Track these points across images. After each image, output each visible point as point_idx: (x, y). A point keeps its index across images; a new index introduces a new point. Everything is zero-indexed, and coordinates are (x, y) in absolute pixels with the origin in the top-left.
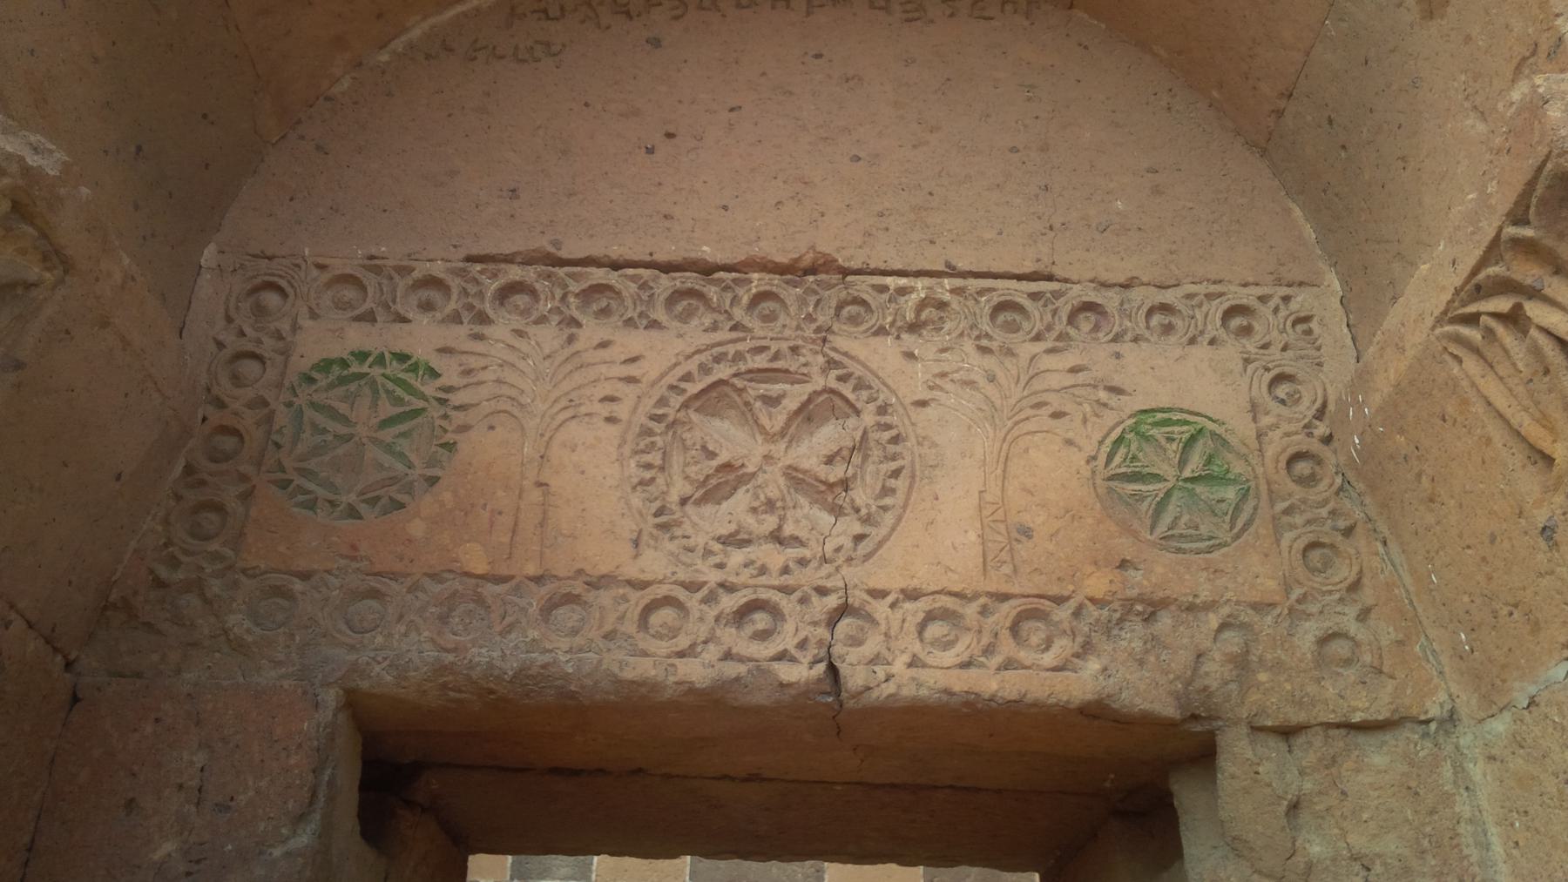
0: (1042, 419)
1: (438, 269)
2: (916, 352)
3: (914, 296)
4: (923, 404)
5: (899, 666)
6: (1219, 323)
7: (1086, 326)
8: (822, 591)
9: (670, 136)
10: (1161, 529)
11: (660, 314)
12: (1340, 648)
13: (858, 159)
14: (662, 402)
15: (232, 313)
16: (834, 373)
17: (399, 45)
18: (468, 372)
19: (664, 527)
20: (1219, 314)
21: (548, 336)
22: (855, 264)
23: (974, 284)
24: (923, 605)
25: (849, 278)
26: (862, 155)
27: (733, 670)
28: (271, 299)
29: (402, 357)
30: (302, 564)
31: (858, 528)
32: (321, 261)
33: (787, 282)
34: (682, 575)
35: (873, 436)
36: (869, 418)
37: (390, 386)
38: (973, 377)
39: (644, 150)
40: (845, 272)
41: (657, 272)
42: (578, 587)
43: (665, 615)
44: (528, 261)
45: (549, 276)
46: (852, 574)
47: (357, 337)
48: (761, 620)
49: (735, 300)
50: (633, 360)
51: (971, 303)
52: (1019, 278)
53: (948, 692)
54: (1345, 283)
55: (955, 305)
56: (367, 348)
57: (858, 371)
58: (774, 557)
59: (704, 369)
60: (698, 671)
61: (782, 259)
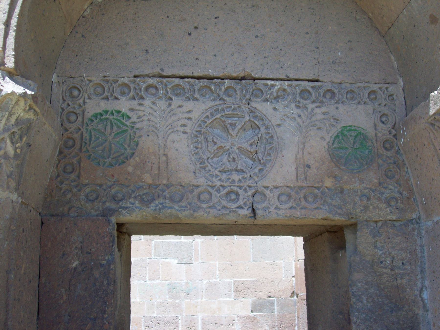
1: (126, 80)
2: (277, 107)
3: (276, 88)
6: (367, 96)
7: (328, 96)
8: (250, 187)
9: (196, 28)
11: (197, 95)
13: (257, 36)
15: (65, 98)
18: (139, 117)
20: (367, 94)
21: (162, 104)
22: (257, 76)
25: (256, 81)
26: (259, 35)
28: (76, 93)
29: (119, 112)
30: (99, 182)
32: (89, 78)
33: (236, 83)
34: (209, 183)
35: (264, 136)
37: (116, 121)
38: (294, 116)
39: (188, 34)
40: (255, 79)
41: (195, 79)
44: (154, 76)
45: (161, 82)
47: (104, 105)
48: (233, 196)
49: (221, 89)
50: (189, 112)
51: (294, 89)
52: (309, 81)
54: (404, 84)
55: (289, 90)
56: (107, 109)
58: (236, 177)
59: (212, 114)
61: (234, 75)
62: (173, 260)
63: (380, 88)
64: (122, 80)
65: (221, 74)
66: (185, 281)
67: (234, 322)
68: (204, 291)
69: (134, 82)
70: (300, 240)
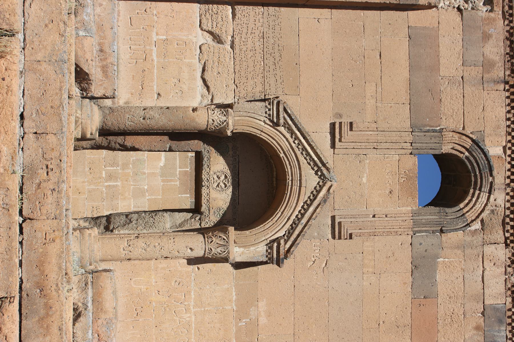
1: (237, 153)
9: (253, 171)
11: (233, 172)
12: (206, 223)
17: (262, 146)
18: (227, 157)
23: (238, 198)
24: (209, 193)
27: (203, 179)
29: (229, 151)
40: (238, 187)
43: (207, 174)
46: (211, 187)
48: (207, 181)
60: (203, 176)
61: (239, 182)
65: (239, 178)
66: (146, 172)
67: (115, 210)
68: (138, 187)
69: (237, 155)
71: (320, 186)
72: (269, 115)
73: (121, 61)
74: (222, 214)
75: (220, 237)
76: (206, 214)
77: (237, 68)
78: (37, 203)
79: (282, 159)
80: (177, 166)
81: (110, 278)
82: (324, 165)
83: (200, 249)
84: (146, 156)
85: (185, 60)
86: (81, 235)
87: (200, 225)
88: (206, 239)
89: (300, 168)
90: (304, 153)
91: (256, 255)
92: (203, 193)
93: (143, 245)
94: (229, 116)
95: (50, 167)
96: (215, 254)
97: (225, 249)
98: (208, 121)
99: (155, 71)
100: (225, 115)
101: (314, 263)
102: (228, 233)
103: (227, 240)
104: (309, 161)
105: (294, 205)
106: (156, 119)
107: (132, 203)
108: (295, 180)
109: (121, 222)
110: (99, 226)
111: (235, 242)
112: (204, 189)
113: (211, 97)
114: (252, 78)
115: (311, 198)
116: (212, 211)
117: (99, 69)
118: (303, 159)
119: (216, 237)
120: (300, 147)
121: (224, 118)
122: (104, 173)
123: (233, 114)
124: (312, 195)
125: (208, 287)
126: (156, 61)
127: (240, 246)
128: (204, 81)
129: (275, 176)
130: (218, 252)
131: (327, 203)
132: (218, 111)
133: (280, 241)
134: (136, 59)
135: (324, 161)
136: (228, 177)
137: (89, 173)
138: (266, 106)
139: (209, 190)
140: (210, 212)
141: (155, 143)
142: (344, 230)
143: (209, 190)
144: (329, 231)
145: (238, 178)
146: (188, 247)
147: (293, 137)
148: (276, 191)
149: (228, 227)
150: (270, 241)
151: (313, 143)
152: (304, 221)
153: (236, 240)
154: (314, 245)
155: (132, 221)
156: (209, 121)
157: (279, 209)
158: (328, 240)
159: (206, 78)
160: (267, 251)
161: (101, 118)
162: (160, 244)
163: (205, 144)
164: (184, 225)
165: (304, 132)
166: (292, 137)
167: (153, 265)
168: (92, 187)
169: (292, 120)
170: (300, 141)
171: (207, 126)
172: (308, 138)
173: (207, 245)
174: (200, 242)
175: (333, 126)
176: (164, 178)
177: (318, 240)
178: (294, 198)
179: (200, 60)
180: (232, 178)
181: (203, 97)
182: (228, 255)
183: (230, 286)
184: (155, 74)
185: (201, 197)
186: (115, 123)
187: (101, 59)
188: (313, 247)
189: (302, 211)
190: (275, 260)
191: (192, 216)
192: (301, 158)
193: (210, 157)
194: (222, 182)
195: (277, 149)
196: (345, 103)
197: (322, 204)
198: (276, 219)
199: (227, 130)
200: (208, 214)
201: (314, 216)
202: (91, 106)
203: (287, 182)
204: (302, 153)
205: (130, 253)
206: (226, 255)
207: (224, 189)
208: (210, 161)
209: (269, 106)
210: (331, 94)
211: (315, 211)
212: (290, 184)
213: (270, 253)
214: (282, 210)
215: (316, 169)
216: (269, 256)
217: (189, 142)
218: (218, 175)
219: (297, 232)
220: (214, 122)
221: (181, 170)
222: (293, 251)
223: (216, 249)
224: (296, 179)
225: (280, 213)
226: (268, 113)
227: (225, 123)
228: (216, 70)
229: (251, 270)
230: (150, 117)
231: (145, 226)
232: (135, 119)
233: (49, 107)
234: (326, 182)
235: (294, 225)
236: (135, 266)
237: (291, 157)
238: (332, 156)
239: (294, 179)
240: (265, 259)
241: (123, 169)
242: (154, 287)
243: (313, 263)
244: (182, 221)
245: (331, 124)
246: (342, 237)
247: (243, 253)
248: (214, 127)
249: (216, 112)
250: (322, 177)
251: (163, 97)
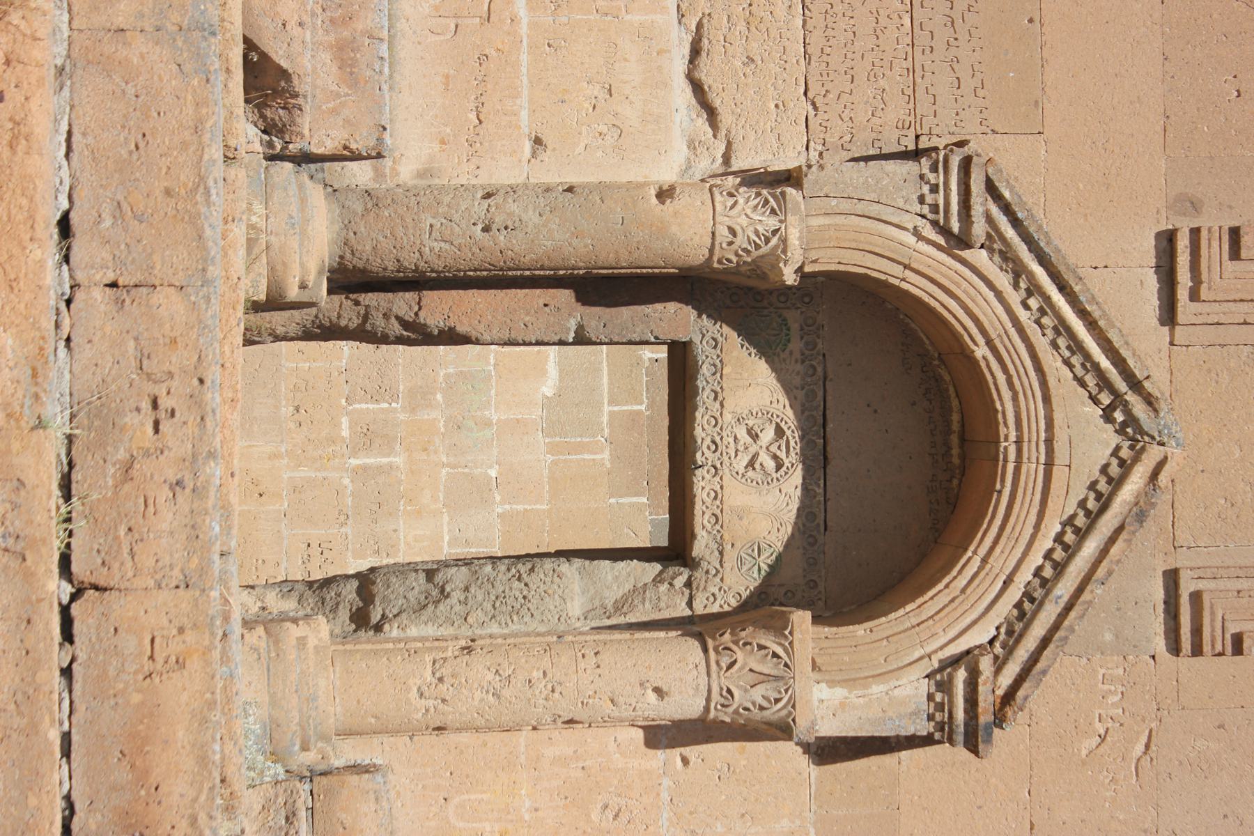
0: (776, 525)
1: (820, 346)
4: (780, 491)
5: (702, 484)
8: (721, 464)
9: (876, 411)
10: (743, 555)
11: (807, 413)
12: (712, 599)
14: (778, 416)
16: (790, 465)
17: (907, 320)
18: (784, 360)
19: (738, 420)
22: (828, 471)
23: (822, 507)
27: (699, 441)
29: (789, 341)
31: (740, 473)
34: (725, 427)
36: (774, 475)
40: (825, 468)
42: (720, 398)
46: (727, 471)
47: (795, 327)
48: (713, 447)
53: (695, 496)
57: (790, 473)
60: (698, 432)
61: (828, 449)
62: (550, 383)
63: (820, 592)
64: (820, 341)
65: (827, 433)
66: (495, 419)
67: (385, 555)
68: (466, 470)
69: (818, 354)
70: (666, 544)
71: (1122, 463)
72: (935, 208)
73: (401, 25)
74: (769, 566)
75: (761, 647)
76: (711, 567)
77: (816, 40)
78: (122, 531)
79: (983, 364)
80: (602, 395)
81: (372, 796)
82: (1135, 384)
83: (691, 692)
84: (492, 362)
85: (629, 17)
86: (271, 644)
87: (690, 604)
88: (712, 654)
89: (1047, 399)
90: (1062, 342)
91: (890, 714)
92: (697, 489)
93: (490, 676)
94: (789, 215)
95: (165, 403)
96: (746, 709)
97: (780, 692)
98: (713, 233)
99: (524, 58)
100: (773, 211)
101: (1103, 740)
102: (791, 633)
103: (786, 659)
104: (1079, 371)
105: (1029, 530)
106: (529, 230)
107: (446, 529)
108: (1029, 441)
109: (411, 595)
110: (335, 609)
111: (814, 666)
112: (703, 478)
113: (723, 148)
114: (872, 76)
115: (1091, 504)
116: (731, 556)
117: (326, 57)
118: (1059, 364)
119: (748, 647)
120: (1046, 321)
121: (772, 222)
122: (345, 422)
123: (803, 207)
124: (1092, 495)
125: (720, 829)
126: (525, 21)
127: (833, 681)
128: (698, 88)
129: (956, 426)
130: (754, 703)
131: (1149, 523)
132: (749, 197)
133: (977, 663)
134: (456, 16)
135: (1137, 373)
136: (788, 433)
137: (292, 425)
138: (922, 177)
139: (721, 479)
140: (726, 558)
141: (528, 314)
142: (1213, 620)
143: (721, 479)
144: (1157, 624)
145: (824, 438)
146: (648, 685)
147: (1023, 285)
148: (961, 481)
149: (790, 612)
150: (940, 661)
151: (1095, 307)
152: (1064, 589)
153: (818, 661)
154: (1100, 677)
155: (449, 594)
156: (717, 234)
157: (972, 548)
158: (1153, 657)
159: (703, 78)
160: (930, 697)
161: (336, 227)
162: (549, 675)
163: (704, 316)
164: (632, 607)
165: (1062, 269)
166: (1016, 286)
167: (523, 749)
168: (305, 472)
169: (1016, 222)
170: (1047, 299)
171: (711, 251)
172: (1077, 288)
173: (714, 675)
174: (691, 666)
175: (1167, 241)
176: (558, 439)
177: (1115, 658)
178: (1026, 505)
179: (683, 16)
180: (802, 438)
181: (695, 148)
182: (790, 713)
183: (798, 822)
184: (524, 70)
185: (693, 504)
186: (386, 245)
187: (332, 21)
188: (1100, 685)
189: (1059, 555)
190: (962, 729)
191: (661, 572)
192: (1053, 363)
193: (721, 361)
194: (764, 449)
195: (963, 332)
196: (1212, 158)
197: (1132, 528)
198: (962, 582)
199: (781, 265)
200: (718, 567)
201: (1101, 572)
202: (301, 187)
203: (1002, 449)
204: (1054, 345)
205: (441, 706)
206: (784, 712)
207: (774, 475)
208: (721, 377)
209: (931, 177)
210: (1159, 129)
211: (1104, 552)
212: (1012, 456)
213: (942, 704)
214: (983, 551)
215: (1106, 399)
216: (937, 714)
217: (647, 309)
218: (750, 425)
219: (1038, 630)
220: (734, 234)
221: (616, 409)
222: (1026, 698)
223: (746, 691)
224: (1034, 438)
225: (977, 561)
226: (929, 199)
227: (774, 241)
228: (741, 50)
229: (874, 768)
230: (510, 224)
231: (495, 609)
232: (457, 229)
233: (159, 193)
234: (1143, 449)
235: (1027, 605)
236: (462, 752)
237: (1015, 357)
238: (1165, 354)
239: (1026, 438)
240: (923, 727)
241: (413, 410)
242: (529, 826)
243: (1099, 740)
244: (626, 591)
245: (1158, 235)
246: (1207, 648)
247: (842, 705)
248: (737, 255)
249: (741, 201)
250: (1130, 428)
251: (554, 149)
